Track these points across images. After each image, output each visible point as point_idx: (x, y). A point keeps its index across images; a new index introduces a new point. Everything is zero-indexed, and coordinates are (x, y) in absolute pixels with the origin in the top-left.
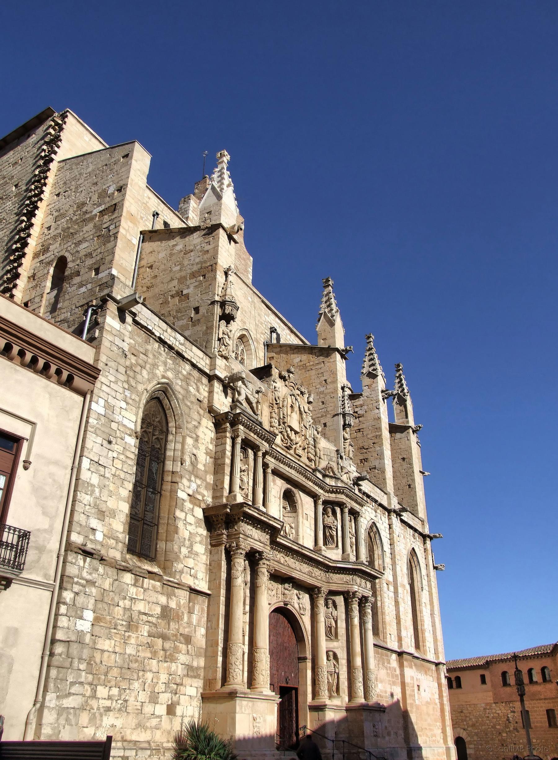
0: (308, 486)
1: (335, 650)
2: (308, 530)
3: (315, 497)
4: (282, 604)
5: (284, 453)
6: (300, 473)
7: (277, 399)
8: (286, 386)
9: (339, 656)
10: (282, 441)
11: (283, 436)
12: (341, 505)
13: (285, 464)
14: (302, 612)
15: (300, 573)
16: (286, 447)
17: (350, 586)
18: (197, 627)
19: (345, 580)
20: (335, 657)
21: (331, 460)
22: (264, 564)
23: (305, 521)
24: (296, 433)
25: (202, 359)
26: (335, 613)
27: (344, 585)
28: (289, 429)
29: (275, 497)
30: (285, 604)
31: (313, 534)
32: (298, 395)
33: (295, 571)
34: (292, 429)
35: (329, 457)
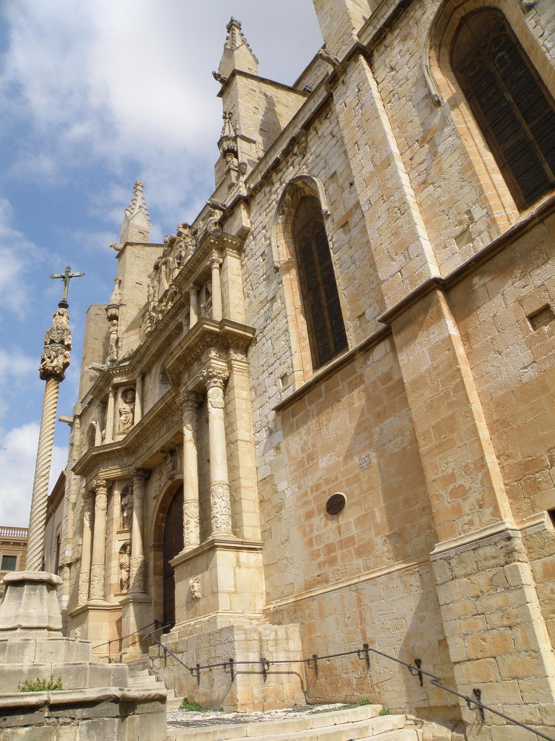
4: (170, 483)
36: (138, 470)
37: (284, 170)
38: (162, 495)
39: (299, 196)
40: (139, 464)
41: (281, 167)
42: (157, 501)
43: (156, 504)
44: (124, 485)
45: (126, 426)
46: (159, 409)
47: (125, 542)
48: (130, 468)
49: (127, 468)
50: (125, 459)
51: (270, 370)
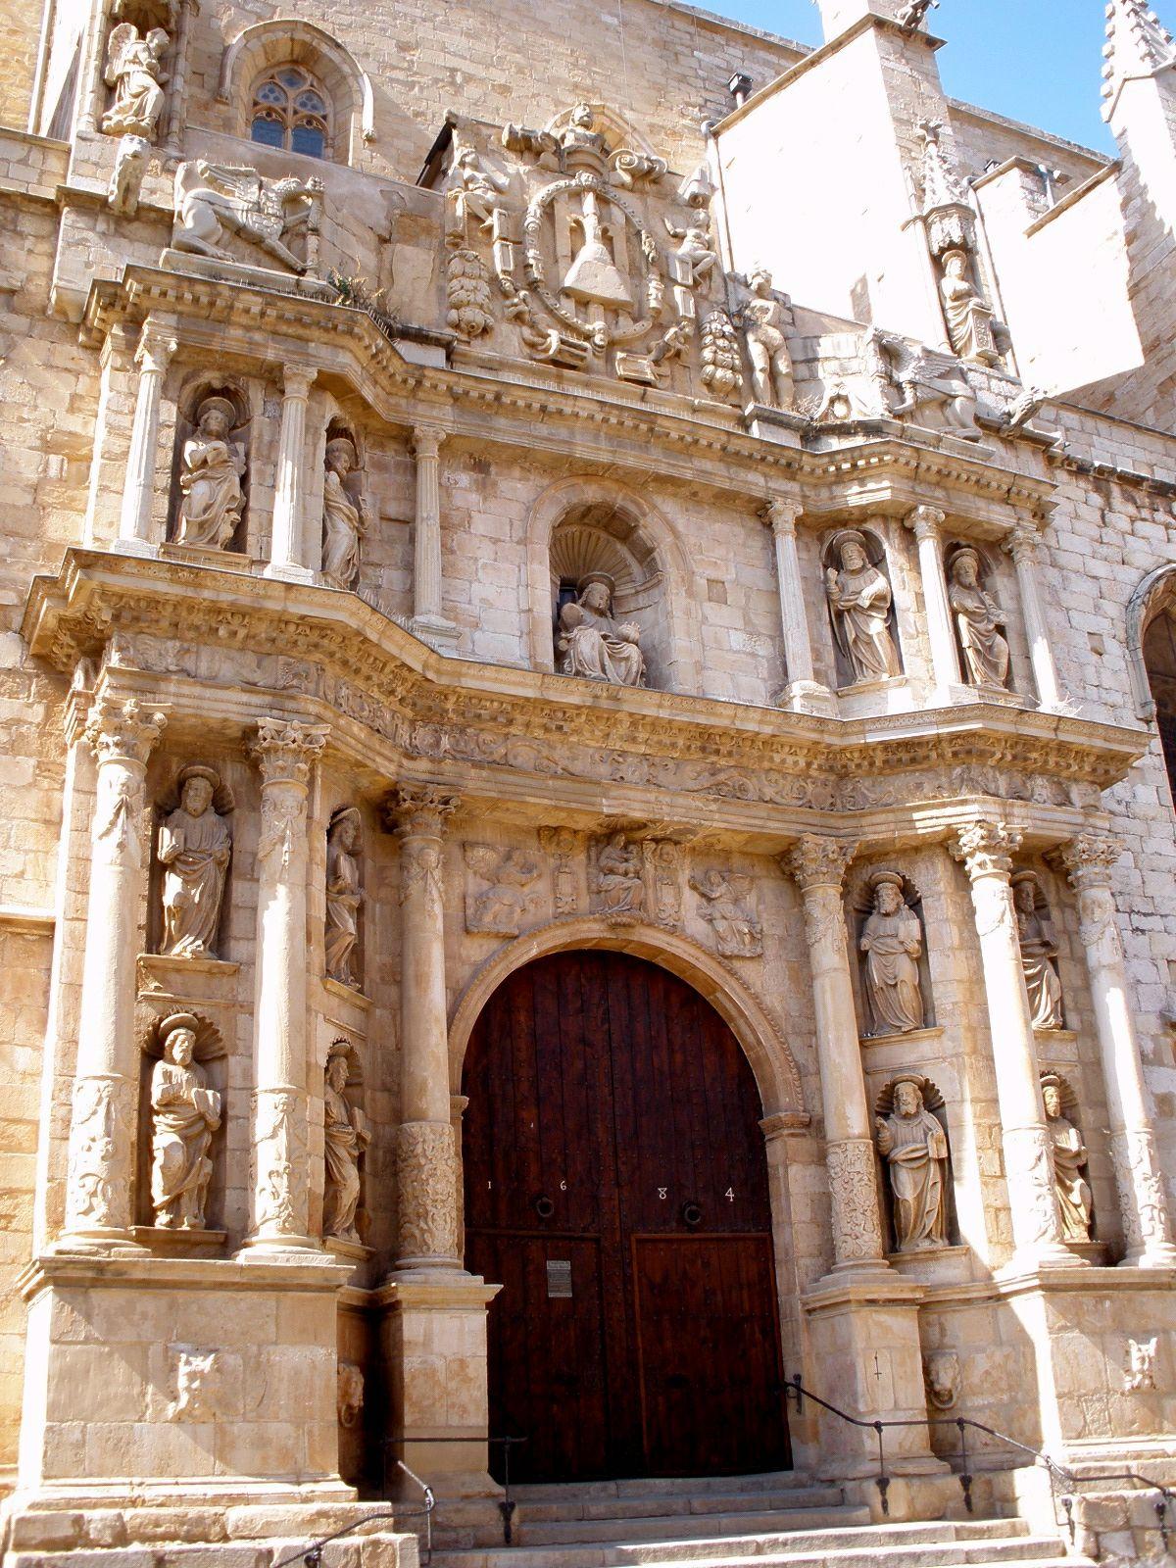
2: (737, 640)
5: (552, 386)
7: (483, 214)
8: (546, 168)
9: (945, 1092)
10: (532, 346)
11: (533, 326)
14: (730, 948)
16: (555, 362)
24: (613, 309)
25: (24, 162)
26: (909, 927)
28: (567, 308)
29: (496, 541)
31: (764, 649)
34: (583, 302)
38: (532, 951)
48: (405, 762)
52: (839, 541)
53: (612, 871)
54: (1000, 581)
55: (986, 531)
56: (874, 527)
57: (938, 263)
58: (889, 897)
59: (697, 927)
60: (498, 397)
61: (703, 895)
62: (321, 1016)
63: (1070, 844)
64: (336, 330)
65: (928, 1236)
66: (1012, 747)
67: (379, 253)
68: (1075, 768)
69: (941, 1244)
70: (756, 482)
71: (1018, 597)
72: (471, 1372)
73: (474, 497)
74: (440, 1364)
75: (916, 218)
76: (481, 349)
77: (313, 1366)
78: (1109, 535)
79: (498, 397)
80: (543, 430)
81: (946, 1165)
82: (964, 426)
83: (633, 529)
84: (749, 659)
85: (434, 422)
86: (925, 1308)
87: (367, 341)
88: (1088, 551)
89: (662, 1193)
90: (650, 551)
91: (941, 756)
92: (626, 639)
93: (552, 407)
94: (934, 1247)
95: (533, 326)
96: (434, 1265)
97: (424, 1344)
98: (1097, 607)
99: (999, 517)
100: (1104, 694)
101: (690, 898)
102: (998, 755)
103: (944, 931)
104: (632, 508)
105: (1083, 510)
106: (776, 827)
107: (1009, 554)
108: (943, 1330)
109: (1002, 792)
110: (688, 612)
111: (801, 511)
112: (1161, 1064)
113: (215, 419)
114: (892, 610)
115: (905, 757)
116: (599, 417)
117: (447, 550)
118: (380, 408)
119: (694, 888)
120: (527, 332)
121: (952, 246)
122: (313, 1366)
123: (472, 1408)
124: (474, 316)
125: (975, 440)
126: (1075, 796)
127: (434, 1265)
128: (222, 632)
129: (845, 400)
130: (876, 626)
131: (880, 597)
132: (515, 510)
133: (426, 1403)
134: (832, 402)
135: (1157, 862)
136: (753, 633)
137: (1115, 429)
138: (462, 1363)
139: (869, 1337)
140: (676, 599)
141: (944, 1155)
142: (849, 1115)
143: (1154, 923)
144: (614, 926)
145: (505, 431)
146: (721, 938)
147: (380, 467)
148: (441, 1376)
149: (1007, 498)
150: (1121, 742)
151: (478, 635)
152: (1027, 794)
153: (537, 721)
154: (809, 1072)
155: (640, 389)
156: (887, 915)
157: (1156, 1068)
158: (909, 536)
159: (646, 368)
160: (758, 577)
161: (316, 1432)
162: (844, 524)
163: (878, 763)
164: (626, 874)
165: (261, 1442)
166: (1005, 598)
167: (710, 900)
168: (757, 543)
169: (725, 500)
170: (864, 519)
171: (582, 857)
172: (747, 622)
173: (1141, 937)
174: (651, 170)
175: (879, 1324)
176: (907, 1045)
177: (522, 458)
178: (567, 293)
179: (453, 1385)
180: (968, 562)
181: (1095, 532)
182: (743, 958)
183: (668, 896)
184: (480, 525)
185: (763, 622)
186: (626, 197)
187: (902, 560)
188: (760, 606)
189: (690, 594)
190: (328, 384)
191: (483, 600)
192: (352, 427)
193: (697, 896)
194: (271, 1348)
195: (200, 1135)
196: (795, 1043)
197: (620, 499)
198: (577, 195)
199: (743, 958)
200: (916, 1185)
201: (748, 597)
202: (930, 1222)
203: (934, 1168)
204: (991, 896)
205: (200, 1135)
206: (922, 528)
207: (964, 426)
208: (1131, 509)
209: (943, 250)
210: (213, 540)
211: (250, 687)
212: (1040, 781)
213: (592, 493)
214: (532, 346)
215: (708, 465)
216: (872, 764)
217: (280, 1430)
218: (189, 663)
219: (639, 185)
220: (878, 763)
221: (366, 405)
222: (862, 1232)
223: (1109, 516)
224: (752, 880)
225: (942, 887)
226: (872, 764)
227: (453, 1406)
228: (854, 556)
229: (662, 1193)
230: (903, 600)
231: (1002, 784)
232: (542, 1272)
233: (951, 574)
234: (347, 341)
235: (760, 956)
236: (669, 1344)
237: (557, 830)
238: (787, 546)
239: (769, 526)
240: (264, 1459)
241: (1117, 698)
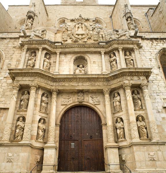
0: (89, 50)
1: (120, 117)
2: (97, 68)
3: (100, 53)
4: (77, 103)
6: (81, 47)
7: (67, 28)
8: (75, 22)
10: (72, 41)
11: (72, 39)
12: (117, 49)
13: (68, 48)
14: (96, 103)
15: (82, 87)
16: (75, 42)
17: (122, 82)
18: (3, 122)
19: (119, 81)
20: (122, 120)
21: (111, 35)
22: (32, 88)
23: (94, 65)
24: (82, 35)
27: (119, 83)
28: (77, 36)
29: (66, 62)
30: (80, 102)
31: (100, 68)
32: (84, 22)
33: (78, 87)
34: (78, 35)
35: (110, 35)
36: (59, 90)
37: (159, 42)
38: (70, 106)
39: (164, 53)
40: (60, 88)
41: (158, 41)
42: (66, 107)
43: (65, 108)
44: (43, 92)
45: (47, 68)
46: (92, 77)
47: (41, 117)
48: (52, 87)
49: (50, 86)
50: (49, 82)
51: (157, 94)
52: (110, 53)
53: (79, 96)
54: (133, 54)
55: (130, 49)
56: (114, 52)
57: (127, 20)
58: (116, 95)
59: (91, 101)
60: (66, 47)
61: (92, 98)
62: (38, 115)
63: (141, 84)
64: (44, 44)
65: (122, 138)
66: (129, 73)
67: (55, 35)
68: (140, 74)
69: (123, 139)
70: (99, 50)
71: (135, 56)
72: (52, 157)
73: (64, 58)
74: (48, 156)
75: (124, 16)
76: (66, 42)
77: (25, 155)
78: (152, 46)
79: (66, 47)
80: (71, 49)
81: (123, 128)
82: (127, 37)
83: (84, 58)
84: (99, 70)
85: (58, 51)
86: (119, 148)
87: (48, 43)
88: (149, 49)
89: (87, 134)
90: (87, 60)
91: (120, 76)
92: (82, 70)
93: (72, 46)
94: (122, 140)
95: (72, 39)
96: (49, 143)
97: (47, 153)
98: (151, 55)
99: (131, 46)
100: (152, 66)
101: (90, 98)
102: (128, 74)
103: (122, 98)
104: (84, 56)
105: (149, 44)
106: (99, 88)
107: (134, 51)
108: (124, 151)
109: (129, 79)
110: (90, 66)
111: (104, 51)
112: (163, 113)
113: (33, 55)
114: (116, 60)
115: (116, 77)
116: (78, 46)
117: (59, 64)
118: (52, 51)
119: (91, 97)
120: (72, 40)
121: (128, 17)
122: (25, 155)
123: (52, 161)
124: (65, 39)
125: (130, 38)
126: (141, 78)
127: (49, 143)
128: (26, 75)
129: (111, 38)
130: (114, 63)
131: (115, 59)
132: (69, 59)
133: (46, 160)
134: (110, 38)
135: (161, 86)
136: (99, 67)
137: (154, 33)
138: (51, 156)
139: (110, 152)
140: (89, 65)
141: (123, 127)
142: (110, 122)
143: (161, 94)
144: (80, 102)
145: (67, 50)
146: (94, 102)
147: (54, 57)
148: (48, 157)
149: (132, 44)
150: (147, 70)
151: (63, 72)
152: (133, 79)
153: (67, 80)
154: (105, 118)
155: (85, 43)
156: (116, 97)
157: (162, 114)
158: (119, 51)
159: (86, 40)
160: (100, 60)
161: (24, 164)
162: (111, 52)
163: (112, 78)
164: (81, 96)
165: (17, 165)
166: (133, 56)
167: (93, 98)
168: (100, 56)
169: (95, 53)
170: (113, 51)
171: (76, 95)
172: (98, 65)
173: (158, 96)
174: (87, 19)
175: (112, 151)
176: (119, 113)
177: (70, 53)
178: (76, 34)
179: (50, 158)
180: (128, 53)
181: (151, 46)
182: (97, 105)
183: (87, 98)
184: (65, 61)
185: (100, 65)
186: (84, 23)
187: (118, 54)
188: (100, 63)
189: (91, 64)
190: (44, 49)
191: (65, 68)
192: (50, 53)
193: (91, 98)
194: (20, 153)
195: (21, 129)
196: (104, 114)
197: (82, 55)
198: (78, 24)
199: (97, 105)
200: (119, 131)
201: (98, 63)
202: (122, 136)
203: (122, 129)
204: (129, 92)
205: (21, 129)
206: (120, 50)
207: (127, 37)
208: (157, 42)
209: (127, 18)
210: (30, 67)
211: (29, 81)
212: (135, 77)
213: (79, 55)
214: (72, 41)
215: (92, 49)
216: (112, 79)
217: (20, 164)
218: (23, 79)
219: (86, 21)
220: (112, 78)
221: (50, 51)
222: (111, 139)
223: (153, 44)
224: (99, 95)
225: (122, 93)
226: (112, 79)
227: (50, 161)
228: (112, 55)
229: (87, 134)
230: (118, 59)
231: (129, 78)
232: (71, 145)
233: (125, 55)
234: (45, 44)
235: (100, 104)
236: (87, 154)
237: (73, 92)
238: (103, 56)
239: (101, 54)
240: (17, 167)
241: (154, 66)
